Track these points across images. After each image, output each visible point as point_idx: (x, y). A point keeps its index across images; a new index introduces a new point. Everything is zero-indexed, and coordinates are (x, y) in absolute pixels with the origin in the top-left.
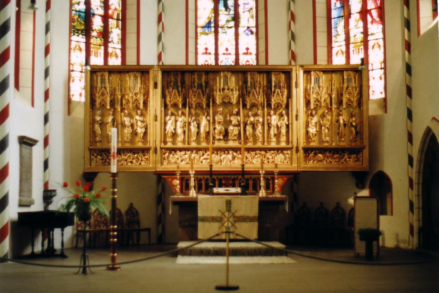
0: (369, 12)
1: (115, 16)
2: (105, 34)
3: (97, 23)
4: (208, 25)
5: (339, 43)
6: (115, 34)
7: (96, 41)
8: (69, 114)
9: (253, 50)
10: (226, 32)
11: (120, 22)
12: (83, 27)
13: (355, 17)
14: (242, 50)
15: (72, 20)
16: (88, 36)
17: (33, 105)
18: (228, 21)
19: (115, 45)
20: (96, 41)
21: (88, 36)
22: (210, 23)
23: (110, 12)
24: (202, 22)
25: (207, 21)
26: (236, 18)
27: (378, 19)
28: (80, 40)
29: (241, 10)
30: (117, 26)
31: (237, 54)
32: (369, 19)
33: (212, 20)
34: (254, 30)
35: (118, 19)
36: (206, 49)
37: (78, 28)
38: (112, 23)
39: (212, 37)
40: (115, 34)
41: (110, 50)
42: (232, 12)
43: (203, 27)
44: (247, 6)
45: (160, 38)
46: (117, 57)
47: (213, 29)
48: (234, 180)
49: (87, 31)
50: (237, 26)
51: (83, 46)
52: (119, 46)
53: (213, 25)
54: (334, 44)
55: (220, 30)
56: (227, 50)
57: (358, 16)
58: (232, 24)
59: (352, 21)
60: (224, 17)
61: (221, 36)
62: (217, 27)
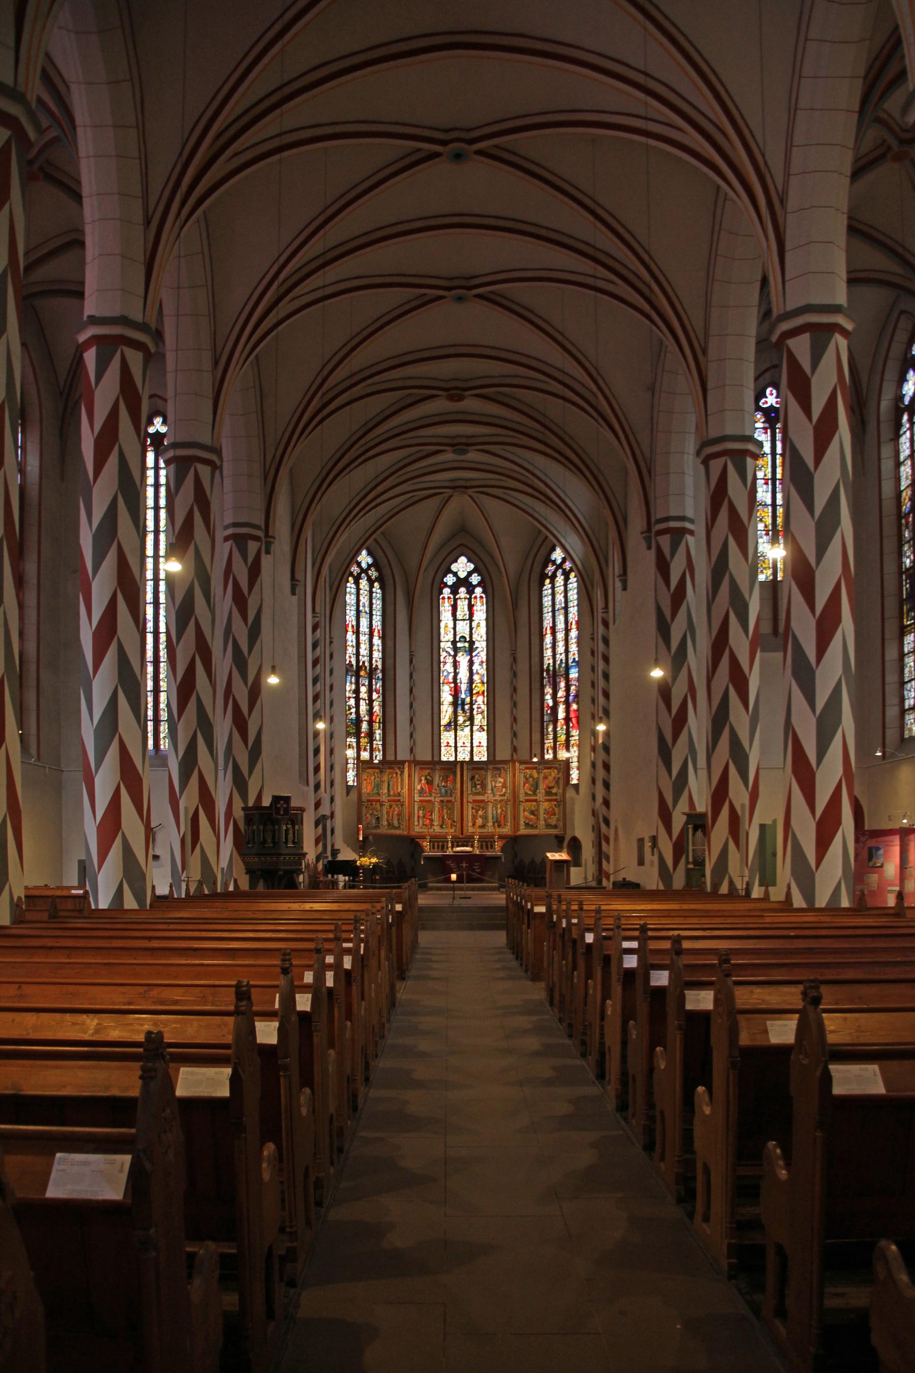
4: (449, 724)
18: (465, 721)
24: (444, 721)
30: (379, 728)
33: (452, 720)
34: (485, 728)
39: (452, 733)
45: (411, 736)
48: (467, 842)
50: (472, 725)
58: (468, 723)
62: (456, 725)
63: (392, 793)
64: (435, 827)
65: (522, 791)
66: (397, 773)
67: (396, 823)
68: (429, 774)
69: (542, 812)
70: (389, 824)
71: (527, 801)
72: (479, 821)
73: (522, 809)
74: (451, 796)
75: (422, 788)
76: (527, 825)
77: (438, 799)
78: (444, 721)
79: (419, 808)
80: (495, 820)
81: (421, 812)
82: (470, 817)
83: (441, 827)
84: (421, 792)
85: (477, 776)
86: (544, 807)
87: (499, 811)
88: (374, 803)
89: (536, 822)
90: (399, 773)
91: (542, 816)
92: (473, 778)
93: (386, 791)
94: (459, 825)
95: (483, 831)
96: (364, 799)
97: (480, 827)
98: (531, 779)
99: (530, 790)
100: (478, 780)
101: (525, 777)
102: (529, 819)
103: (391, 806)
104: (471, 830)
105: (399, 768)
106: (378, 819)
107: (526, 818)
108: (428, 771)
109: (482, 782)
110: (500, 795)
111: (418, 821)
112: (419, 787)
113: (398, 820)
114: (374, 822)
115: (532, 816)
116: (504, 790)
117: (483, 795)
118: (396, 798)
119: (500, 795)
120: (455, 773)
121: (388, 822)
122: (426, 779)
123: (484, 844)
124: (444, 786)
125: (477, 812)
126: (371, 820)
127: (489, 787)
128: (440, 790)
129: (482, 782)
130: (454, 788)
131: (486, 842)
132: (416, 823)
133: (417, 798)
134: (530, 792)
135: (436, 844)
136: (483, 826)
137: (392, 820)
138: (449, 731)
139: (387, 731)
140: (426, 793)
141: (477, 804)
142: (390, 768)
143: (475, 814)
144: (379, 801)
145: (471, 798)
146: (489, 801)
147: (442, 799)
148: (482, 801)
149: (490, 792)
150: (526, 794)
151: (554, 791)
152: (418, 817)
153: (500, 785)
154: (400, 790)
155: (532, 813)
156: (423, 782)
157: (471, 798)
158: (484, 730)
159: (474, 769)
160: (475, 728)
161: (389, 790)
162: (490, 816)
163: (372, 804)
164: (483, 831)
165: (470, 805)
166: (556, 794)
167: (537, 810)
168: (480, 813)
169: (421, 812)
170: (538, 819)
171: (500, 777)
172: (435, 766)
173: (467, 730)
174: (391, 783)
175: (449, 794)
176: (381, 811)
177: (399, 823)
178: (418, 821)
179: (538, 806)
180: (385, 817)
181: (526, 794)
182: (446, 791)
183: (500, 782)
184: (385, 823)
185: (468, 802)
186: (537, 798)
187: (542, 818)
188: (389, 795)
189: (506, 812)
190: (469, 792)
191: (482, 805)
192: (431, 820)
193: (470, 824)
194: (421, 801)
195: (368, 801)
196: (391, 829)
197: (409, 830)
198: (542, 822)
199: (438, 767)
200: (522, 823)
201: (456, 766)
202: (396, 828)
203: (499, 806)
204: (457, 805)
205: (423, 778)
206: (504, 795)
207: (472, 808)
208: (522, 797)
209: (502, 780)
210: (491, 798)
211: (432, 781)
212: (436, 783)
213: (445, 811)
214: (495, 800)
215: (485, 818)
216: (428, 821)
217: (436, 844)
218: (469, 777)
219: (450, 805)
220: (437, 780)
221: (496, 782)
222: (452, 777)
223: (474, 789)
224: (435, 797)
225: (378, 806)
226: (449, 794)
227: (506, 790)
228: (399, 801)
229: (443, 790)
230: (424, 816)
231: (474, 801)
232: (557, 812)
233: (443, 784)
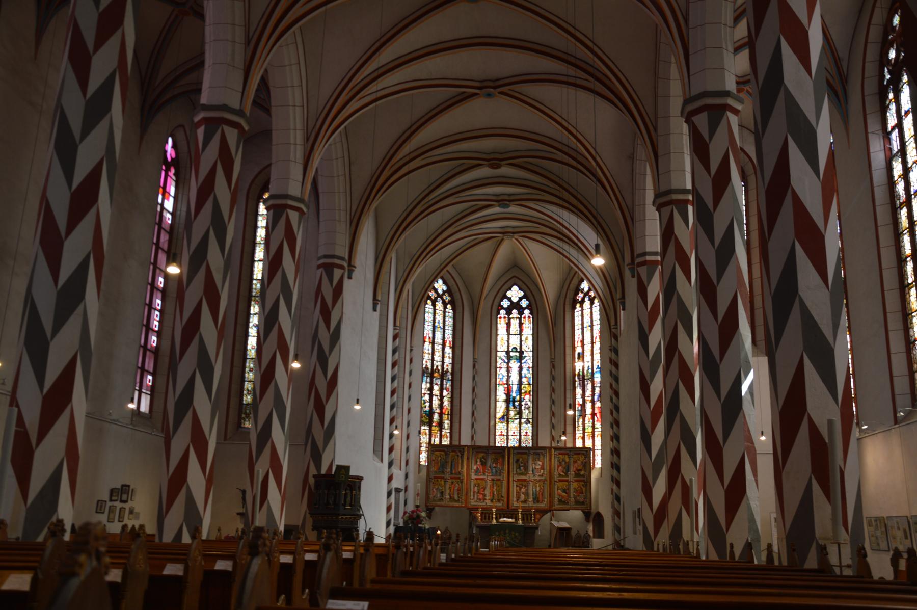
0: (595, 414)
1: (447, 413)
2: (440, 424)
3: (436, 417)
4: (503, 417)
5: (579, 434)
6: (447, 424)
7: (435, 429)
8: (419, 473)
9: (530, 434)
10: (513, 422)
11: (449, 416)
12: (428, 421)
13: (588, 417)
14: (523, 433)
15: (422, 417)
16: (430, 426)
17: (400, 470)
18: (515, 415)
19: (446, 431)
20: (435, 429)
21: (430, 426)
22: (504, 416)
23: (444, 411)
24: (499, 415)
25: (502, 414)
26: (520, 413)
27: (600, 419)
28: (425, 429)
29: (523, 408)
30: (448, 419)
31: (520, 436)
32: (596, 419)
34: (531, 421)
35: (448, 415)
36: (502, 432)
37: (425, 421)
38: (445, 417)
39: (505, 424)
40: (447, 424)
41: (443, 433)
42: (517, 409)
43: (499, 418)
44: (527, 406)
46: (447, 438)
47: (506, 419)
48: (512, 514)
49: (430, 424)
50: (520, 418)
51: (427, 432)
52: (449, 431)
53: (505, 417)
54: (577, 432)
55: (510, 420)
56: (514, 433)
57: (590, 416)
58: (517, 417)
59: (587, 419)
60: (512, 413)
61: (511, 425)
62: (508, 419)
63: (454, 472)
64: (487, 501)
65: (556, 473)
66: (458, 456)
67: (456, 497)
68: (483, 457)
69: (572, 490)
70: (451, 498)
71: (560, 481)
72: (523, 497)
73: (556, 487)
74: (500, 475)
75: (477, 468)
76: (560, 501)
77: (489, 478)
78: (499, 415)
79: (475, 485)
80: (535, 496)
81: (476, 488)
82: (515, 494)
83: (492, 501)
84: (477, 471)
85: (521, 460)
86: (574, 487)
87: (538, 489)
88: (439, 480)
89: (568, 499)
90: (460, 455)
91: (572, 494)
92: (517, 461)
93: (449, 470)
94: (505, 500)
95: (525, 505)
96: (432, 476)
97: (522, 502)
98: (563, 463)
99: (563, 472)
100: (521, 463)
101: (559, 461)
102: (562, 496)
103: (452, 483)
104: (515, 504)
105: (460, 451)
106: (442, 493)
107: (560, 495)
108: (482, 454)
109: (525, 464)
110: (539, 476)
111: (474, 496)
112: (475, 468)
113: (458, 494)
114: (439, 496)
115: (564, 494)
116: (542, 471)
117: (526, 475)
118: (456, 476)
119: (539, 476)
120: (503, 457)
121: (450, 496)
122: (481, 461)
123: (525, 516)
124: (495, 467)
125: (520, 489)
126: (436, 495)
127: (531, 469)
128: (492, 470)
129: (525, 464)
130: (503, 469)
131: (527, 515)
132: (472, 497)
133: (473, 477)
134: (563, 474)
135: (487, 515)
136: (525, 501)
137: (453, 494)
138: (502, 423)
139: (454, 421)
140: (480, 472)
141: (521, 483)
142: (453, 451)
143: (518, 490)
144: (443, 478)
145: (516, 477)
146: (530, 481)
147: (493, 477)
148: (525, 480)
149: (531, 472)
150: (560, 475)
151: (582, 473)
152: (474, 492)
153: (539, 467)
154: (460, 469)
155: (564, 491)
156: (478, 463)
157: (516, 477)
158: (529, 423)
159: (519, 453)
160: (523, 421)
161: (451, 470)
162: (531, 492)
163: (438, 481)
164: (525, 505)
165: (515, 484)
166: (583, 476)
167: (568, 489)
168: (523, 490)
169: (476, 488)
170: (569, 496)
171: (539, 460)
172: (488, 450)
173: (517, 422)
174: (453, 464)
175: (498, 474)
176: (445, 486)
177: (459, 497)
178: (474, 496)
179: (569, 485)
180: (448, 491)
181: (560, 475)
182: (496, 471)
183: (539, 465)
184: (448, 497)
185: (513, 480)
186: (569, 478)
187: (572, 496)
188: (452, 474)
189: (544, 490)
190: (515, 472)
191: (524, 483)
192: (484, 495)
193: (515, 499)
194: (477, 479)
195: (435, 478)
196: (452, 502)
197: (466, 503)
198: (572, 499)
199: (490, 451)
200: (556, 499)
201: (504, 451)
202: (456, 501)
203: (538, 485)
204: (505, 483)
205: (478, 460)
206: (542, 476)
207: (517, 486)
208: (556, 478)
209: (540, 463)
210: (532, 478)
211: (485, 463)
212: (489, 465)
213: (495, 487)
214: (535, 480)
215: (527, 494)
216: (482, 496)
217: (487, 515)
218: (515, 459)
219: (499, 483)
220: (489, 462)
221: (535, 464)
222: (501, 460)
223: (518, 470)
224: (487, 476)
225: (443, 482)
226: (498, 474)
227: (544, 471)
228: (459, 478)
229: (494, 470)
230: (478, 492)
231: (519, 480)
232: (584, 490)
233: (494, 465)
